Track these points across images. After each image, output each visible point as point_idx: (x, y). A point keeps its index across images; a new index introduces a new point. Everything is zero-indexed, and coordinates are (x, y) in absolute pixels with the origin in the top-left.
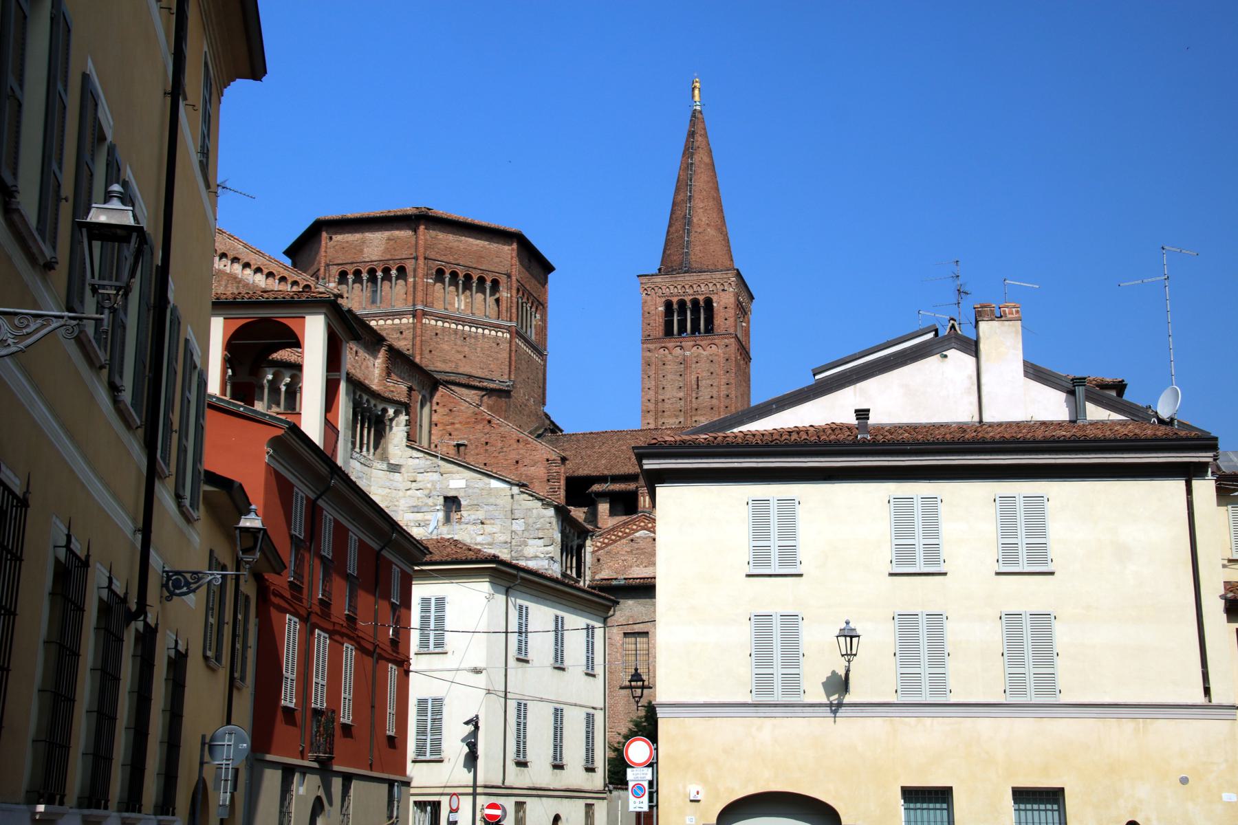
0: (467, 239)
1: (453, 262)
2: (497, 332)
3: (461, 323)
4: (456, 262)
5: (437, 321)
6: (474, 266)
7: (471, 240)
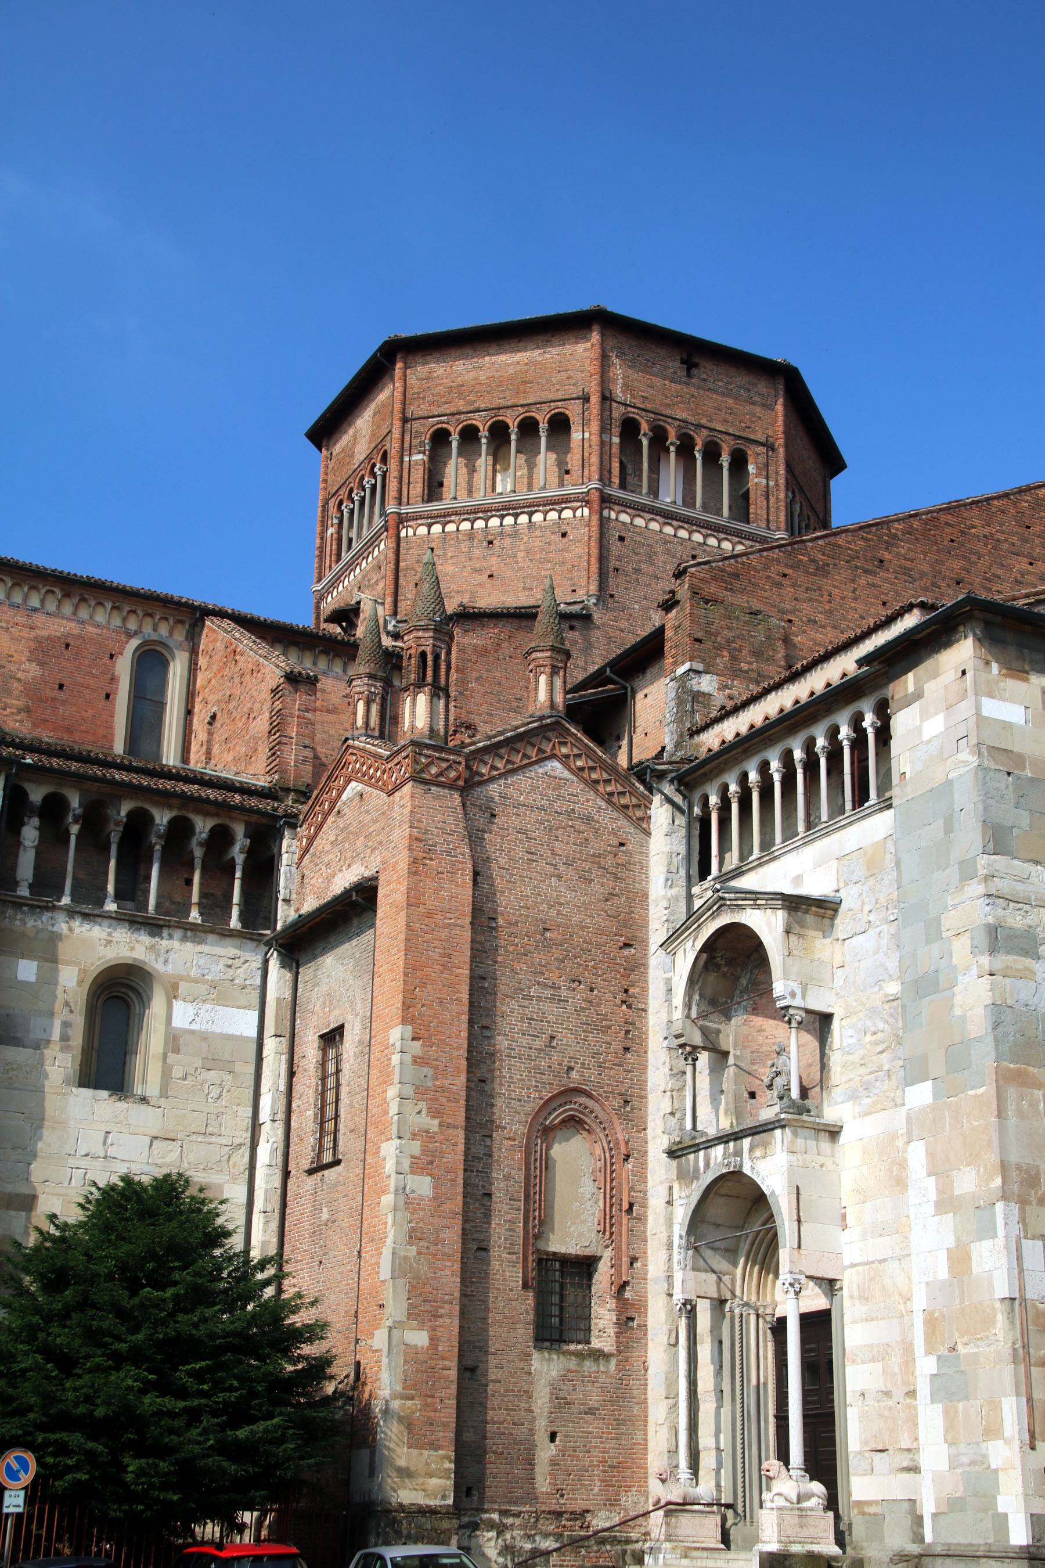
2: (560, 512)
3: (480, 515)
4: (471, 408)
5: (429, 526)
7: (503, 358)
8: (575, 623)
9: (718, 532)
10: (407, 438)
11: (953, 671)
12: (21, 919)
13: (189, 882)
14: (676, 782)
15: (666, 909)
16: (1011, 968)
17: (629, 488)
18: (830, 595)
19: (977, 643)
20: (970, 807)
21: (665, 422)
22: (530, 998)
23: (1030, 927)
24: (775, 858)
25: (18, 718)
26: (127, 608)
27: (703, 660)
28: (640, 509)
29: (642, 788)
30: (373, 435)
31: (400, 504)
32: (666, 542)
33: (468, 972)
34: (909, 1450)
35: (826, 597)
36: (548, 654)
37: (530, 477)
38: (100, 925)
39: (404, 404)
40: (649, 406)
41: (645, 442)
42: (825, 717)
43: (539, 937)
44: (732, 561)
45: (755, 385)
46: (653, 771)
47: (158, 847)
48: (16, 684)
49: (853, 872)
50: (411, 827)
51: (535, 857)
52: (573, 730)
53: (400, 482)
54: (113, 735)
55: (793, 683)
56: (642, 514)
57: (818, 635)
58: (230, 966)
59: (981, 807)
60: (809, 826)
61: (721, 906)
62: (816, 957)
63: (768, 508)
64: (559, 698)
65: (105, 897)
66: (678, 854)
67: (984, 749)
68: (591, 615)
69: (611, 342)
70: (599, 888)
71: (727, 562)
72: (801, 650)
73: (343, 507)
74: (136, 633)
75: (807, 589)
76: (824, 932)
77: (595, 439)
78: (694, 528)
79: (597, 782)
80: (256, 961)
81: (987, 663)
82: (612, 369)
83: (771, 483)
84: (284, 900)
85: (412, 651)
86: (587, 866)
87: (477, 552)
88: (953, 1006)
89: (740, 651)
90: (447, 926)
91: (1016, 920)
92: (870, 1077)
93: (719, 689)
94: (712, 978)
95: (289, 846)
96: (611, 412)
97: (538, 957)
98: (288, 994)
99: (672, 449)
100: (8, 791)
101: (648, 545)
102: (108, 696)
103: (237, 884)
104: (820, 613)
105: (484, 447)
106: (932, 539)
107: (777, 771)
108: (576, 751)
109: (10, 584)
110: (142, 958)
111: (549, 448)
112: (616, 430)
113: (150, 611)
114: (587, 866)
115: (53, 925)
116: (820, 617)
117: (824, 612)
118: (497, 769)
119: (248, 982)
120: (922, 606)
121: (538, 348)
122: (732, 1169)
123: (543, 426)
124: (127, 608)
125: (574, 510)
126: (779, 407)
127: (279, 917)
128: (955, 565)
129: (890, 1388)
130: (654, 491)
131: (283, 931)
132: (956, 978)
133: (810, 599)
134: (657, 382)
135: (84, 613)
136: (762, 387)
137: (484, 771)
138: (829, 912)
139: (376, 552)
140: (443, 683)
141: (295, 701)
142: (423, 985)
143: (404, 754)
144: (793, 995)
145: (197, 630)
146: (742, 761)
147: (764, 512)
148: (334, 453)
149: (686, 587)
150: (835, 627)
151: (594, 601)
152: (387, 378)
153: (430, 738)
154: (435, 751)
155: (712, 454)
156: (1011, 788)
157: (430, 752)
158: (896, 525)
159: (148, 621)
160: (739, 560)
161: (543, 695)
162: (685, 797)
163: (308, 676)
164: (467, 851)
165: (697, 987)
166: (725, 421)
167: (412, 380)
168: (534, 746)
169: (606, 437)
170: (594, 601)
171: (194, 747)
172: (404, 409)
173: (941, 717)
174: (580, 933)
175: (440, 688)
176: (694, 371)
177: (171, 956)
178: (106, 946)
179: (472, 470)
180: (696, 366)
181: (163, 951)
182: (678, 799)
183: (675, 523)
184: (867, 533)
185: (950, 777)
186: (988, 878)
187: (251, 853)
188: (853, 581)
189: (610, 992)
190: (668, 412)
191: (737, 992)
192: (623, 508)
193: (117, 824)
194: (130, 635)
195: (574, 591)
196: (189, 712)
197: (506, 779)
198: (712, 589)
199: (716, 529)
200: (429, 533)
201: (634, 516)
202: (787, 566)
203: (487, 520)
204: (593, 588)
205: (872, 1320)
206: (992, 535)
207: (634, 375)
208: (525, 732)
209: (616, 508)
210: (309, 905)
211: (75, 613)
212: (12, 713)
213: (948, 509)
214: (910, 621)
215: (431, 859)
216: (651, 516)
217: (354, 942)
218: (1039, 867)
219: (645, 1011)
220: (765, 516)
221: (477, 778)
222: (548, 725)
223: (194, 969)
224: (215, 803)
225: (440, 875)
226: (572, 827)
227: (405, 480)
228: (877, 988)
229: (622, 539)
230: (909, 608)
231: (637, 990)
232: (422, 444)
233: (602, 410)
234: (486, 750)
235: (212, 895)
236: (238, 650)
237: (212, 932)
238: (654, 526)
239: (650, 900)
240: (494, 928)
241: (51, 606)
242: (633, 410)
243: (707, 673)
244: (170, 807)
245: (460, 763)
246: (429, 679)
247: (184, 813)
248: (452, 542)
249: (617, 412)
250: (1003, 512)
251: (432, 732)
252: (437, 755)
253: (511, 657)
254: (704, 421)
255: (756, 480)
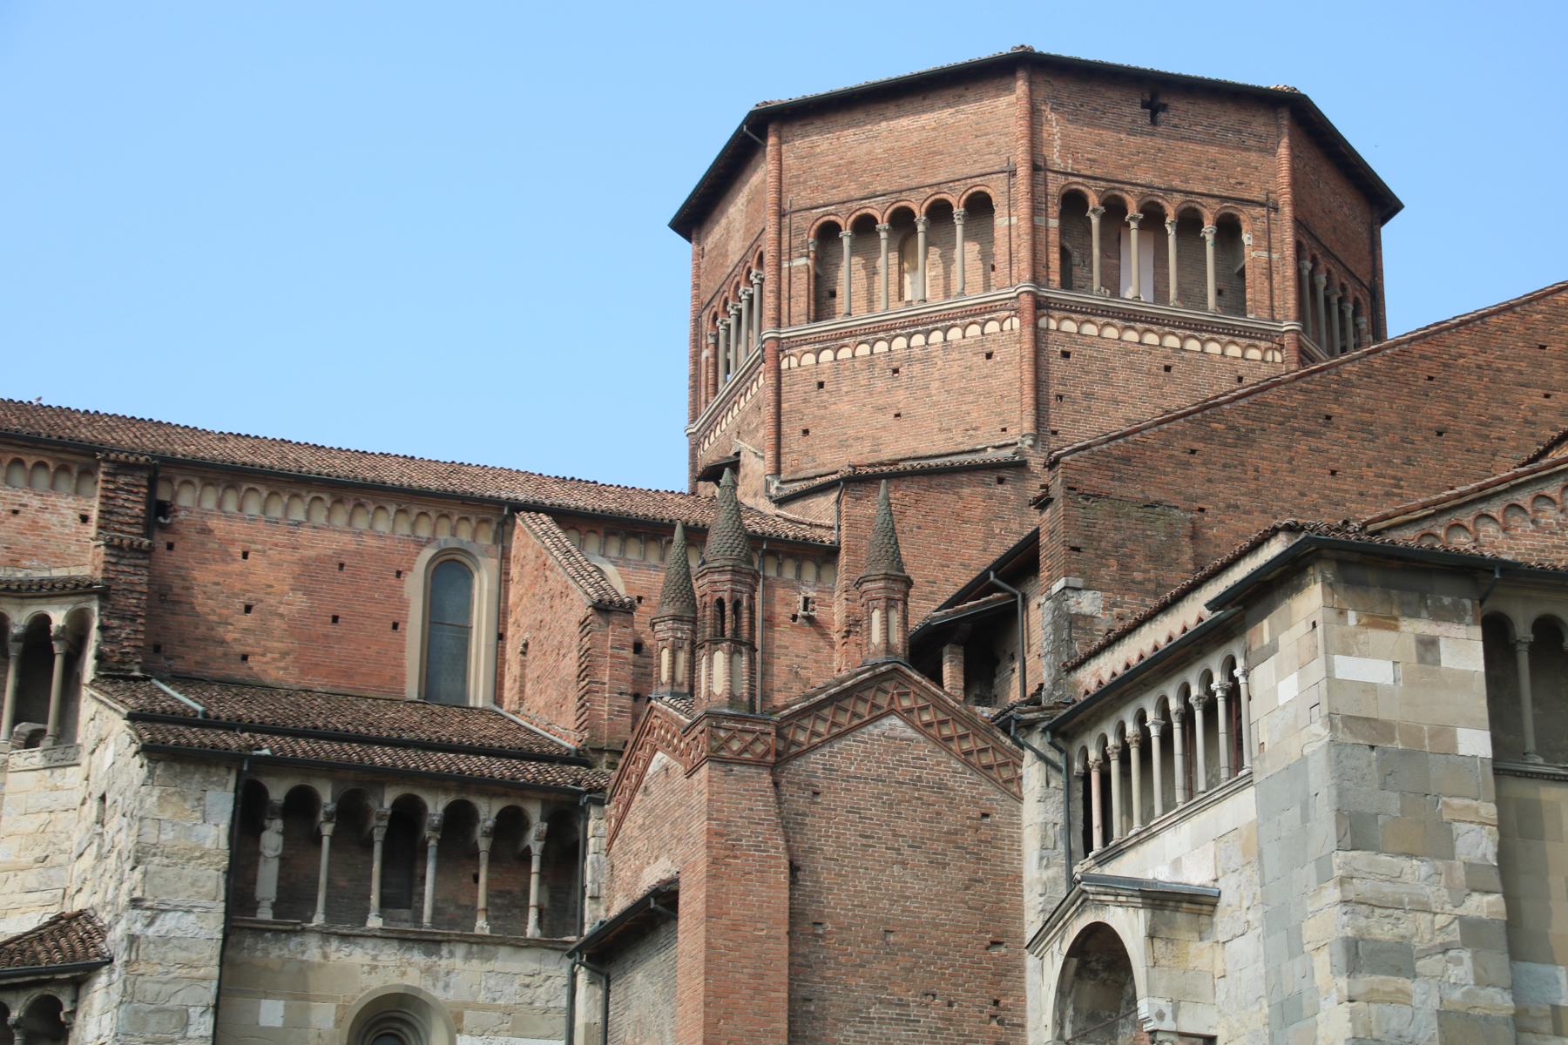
0: (892, 123)
1: (857, 196)
2: (983, 325)
3: (881, 335)
5: (818, 353)
6: (914, 184)
7: (903, 122)
8: (1004, 474)
9: (1201, 331)
10: (785, 237)
11: (1303, 623)
12: (263, 949)
13: (476, 878)
14: (1048, 733)
15: (1041, 895)
16: (1378, 990)
17: (1076, 283)
18: (1256, 470)
19: (1328, 589)
20: (1324, 792)
21: (1122, 190)
22: (869, 1020)
23: (1403, 937)
24: (1153, 835)
25: (282, 664)
26: (416, 511)
27: (1082, 574)
28: (1090, 312)
29: (1008, 742)
30: (748, 230)
31: (779, 326)
32: (1127, 353)
33: (786, 995)
35: (1251, 474)
36: (881, 584)
37: (947, 276)
38: (362, 947)
39: (780, 192)
40: (1098, 172)
41: (1095, 221)
42: (1198, 659)
43: (878, 942)
44: (1121, 441)
45: (1249, 123)
46: (1017, 721)
47: (432, 843)
48: (277, 622)
49: (1230, 858)
50: (709, 819)
51: (871, 841)
52: (916, 677)
53: (779, 298)
54: (403, 675)
55: (1166, 615)
56: (1093, 319)
57: (1240, 524)
58: (528, 986)
59: (1334, 792)
60: (1166, 808)
61: (1085, 900)
62: (1191, 966)
63: (1271, 291)
64: (897, 638)
65: (367, 911)
66: (1055, 824)
67: (1338, 721)
68: (1026, 461)
69: (1043, 91)
70: (955, 874)
71: (1113, 443)
72: (1218, 546)
73: (718, 324)
74: (429, 541)
75: (1225, 466)
76: (1200, 933)
77: (1025, 226)
78: (1167, 329)
79: (950, 739)
80: (561, 979)
81: (1342, 612)
82: (1046, 127)
83: (1275, 256)
84: (590, 897)
85: (707, 599)
86: (939, 846)
87: (880, 385)
88: (1316, 1039)
89: (1132, 557)
90: (758, 939)
91: (1383, 930)
93: (1104, 609)
94: (1088, 987)
95: (596, 827)
96: (1046, 185)
97: (880, 968)
98: (598, 1018)
99: (1133, 225)
100: (240, 792)
101: (1103, 360)
102: (395, 626)
103: (534, 880)
104: (1243, 495)
105: (884, 244)
106: (1401, 379)
107: (1154, 723)
108: (921, 703)
109: (265, 494)
110: (416, 984)
111: (966, 238)
112: (1054, 209)
113: (446, 512)
114: (939, 846)
115: (303, 953)
116: (1243, 501)
117: (1249, 494)
118: (819, 735)
119: (551, 1004)
120: (1289, 529)
121: (949, 106)
123: (958, 210)
124: (416, 511)
125: (1002, 322)
126: (1283, 151)
127: (586, 920)
128: (1435, 411)
130: (1112, 283)
131: (595, 936)
132: (1318, 1003)
133: (1230, 479)
134: (1109, 136)
135: (361, 522)
136: (1259, 124)
137: (802, 739)
138: (1206, 908)
139: (755, 389)
140: (745, 634)
141: (607, 636)
142: (728, 1016)
143: (700, 728)
144: (1161, 1016)
145: (507, 528)
146: (1119, 708)
147: (1266, 297)
148: (706, 250)
149: (1060, 480)
150: (1264, 512)
151: (1029, 442)
152: (759, 155)
153: (731, 706)
154: (737, 721)
155: (1189, 223)
156: (1374, 765)
157: (731, 724)
158: (1349, 367)
159: (444, 522)
160: (1130, 438)
161: (876, 636)
162: (1061, 751)
163: (622, 605)
164: (781, 842)
165: (1069, 1000)
166: (1207, 178)
167: (789, 160)
168: (866, 701)
169: (1039, 221)
170: (1029, 442)
171: (508, 683)
172: (780, 199)
173: (1295, 676)
174: (933, 932)
175: (742, 643)
176: (1162, 116)
177: (453, 979)
178: (370, 973)
179: (872, 272)
180: (1164, 107)
181: (442, 973)
182: (1053, 755)
183: (1139, 326)
184: (1308, 383)
185: (1305, 753)
186: (1342, 881)
187: (549, 838)
188: (1289, 448)
189: (975, 1005)
190: (1126, 176)
191: (1124, 1003)
192: (1066, 314)
193: (380, 818)
194: (421, 544)
195: (1004, 430)
196: (501, 637)
197: (832, 747)
198: (1095, 481)
199: (1197, 327)
200: (817, 362)
201: (1082, 323)
202: (1195, 439)
203: (890, 342)
204: (1028, 425)
206: (1489, 364)
207: (1075, 131)
208: (853, 686)
209: (1057, 314)
210: (619, 904)
211: (350, 524)
212: (274, 659)
213: (1424, 336)
214: (1275, 548)
215: (735, 857)
216: (1106, 320)
217: (662, 957)
218: (1415, 862)
219: (1022, 1026)
220: (1267, 303)
221: (794, 749)
222: (883, 674)
223: (483, 992)
224: (501, 783)
225: (747, 876)
226: (918, 799)
227: (785, 294)
228: (1257, 1007)
229: (1066, 355)
230: (1275, 532)
231: (1011, 1000)
232: (805, 244)
233: (1033, 185)
234: (804, 713)
235: (509, 892)
236: (548, 563)
237: (503, 943)
238: (1111, 333)
239: (1024, 884)
240: (820, 936)
241: (319, 517)
242: (1076, 179)
243: (1088, 589)
244: (446, 790)
245: (769, 734)
246: (728, 633)
247: (463, 796)
248: (847, 373)
249: (1055, 185)
250: (1505, 331)
251: (733, 699)
252: (740, 726)
253: (919, 528)
254: (1177, 183)
255: (1253, 254)
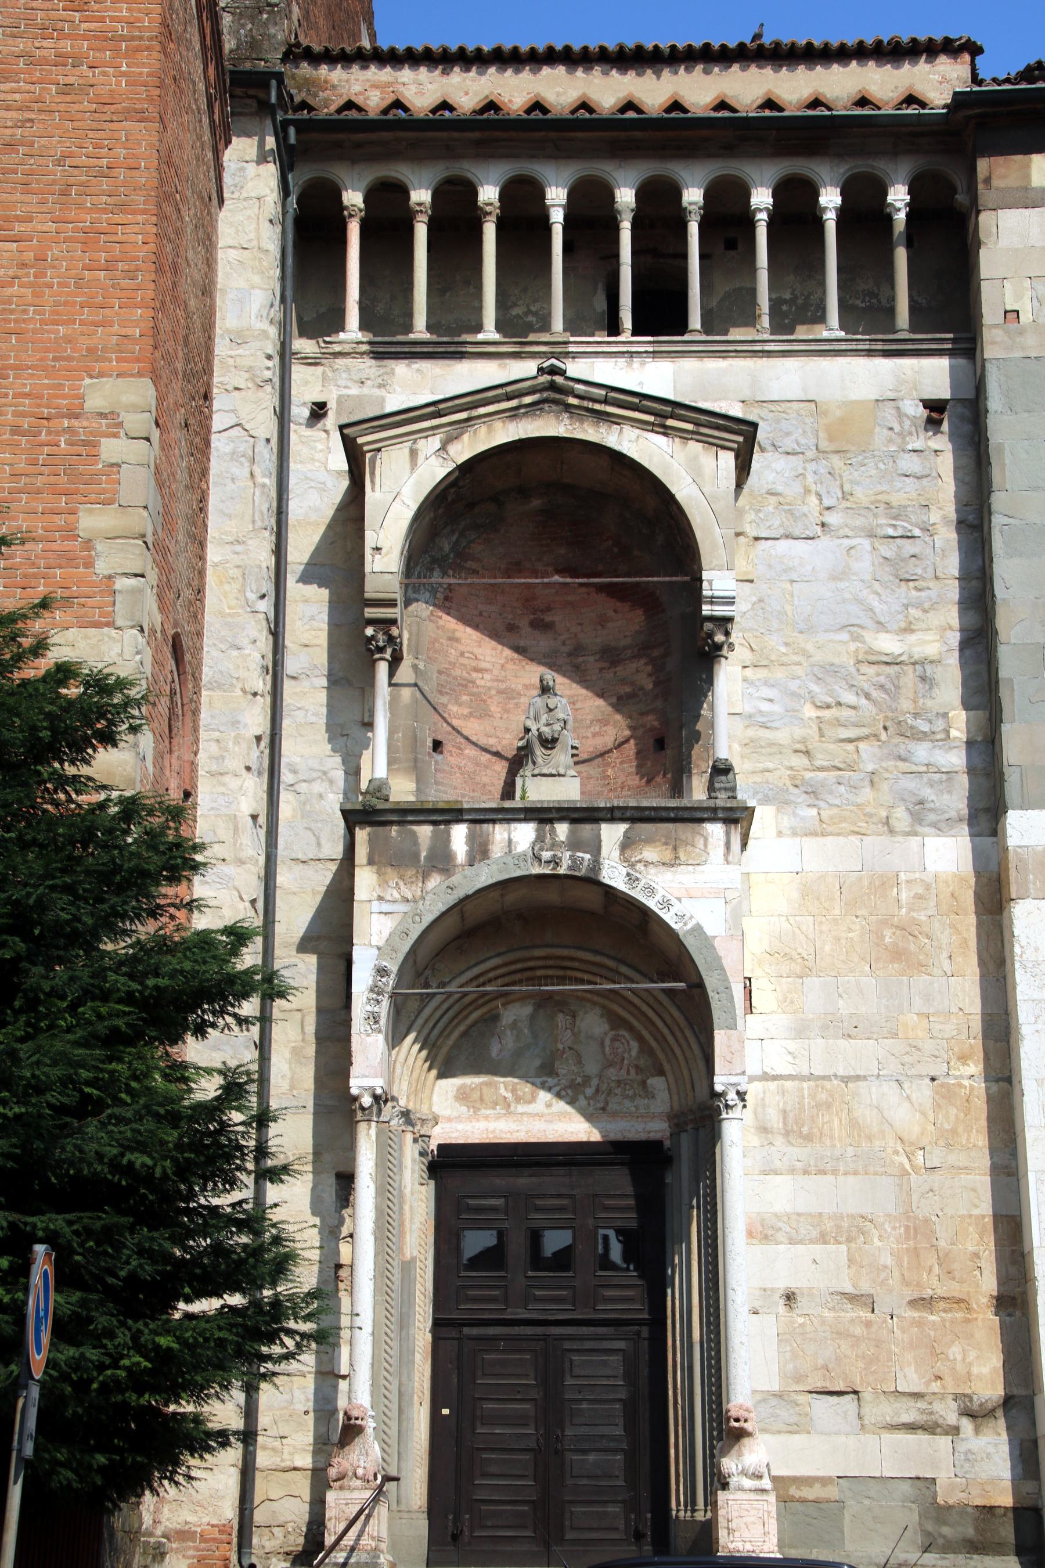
34: (917, 1396)
92: (821, 775)
122: (562, 870)
129: (865, 1287)
205: (823, 1172)
